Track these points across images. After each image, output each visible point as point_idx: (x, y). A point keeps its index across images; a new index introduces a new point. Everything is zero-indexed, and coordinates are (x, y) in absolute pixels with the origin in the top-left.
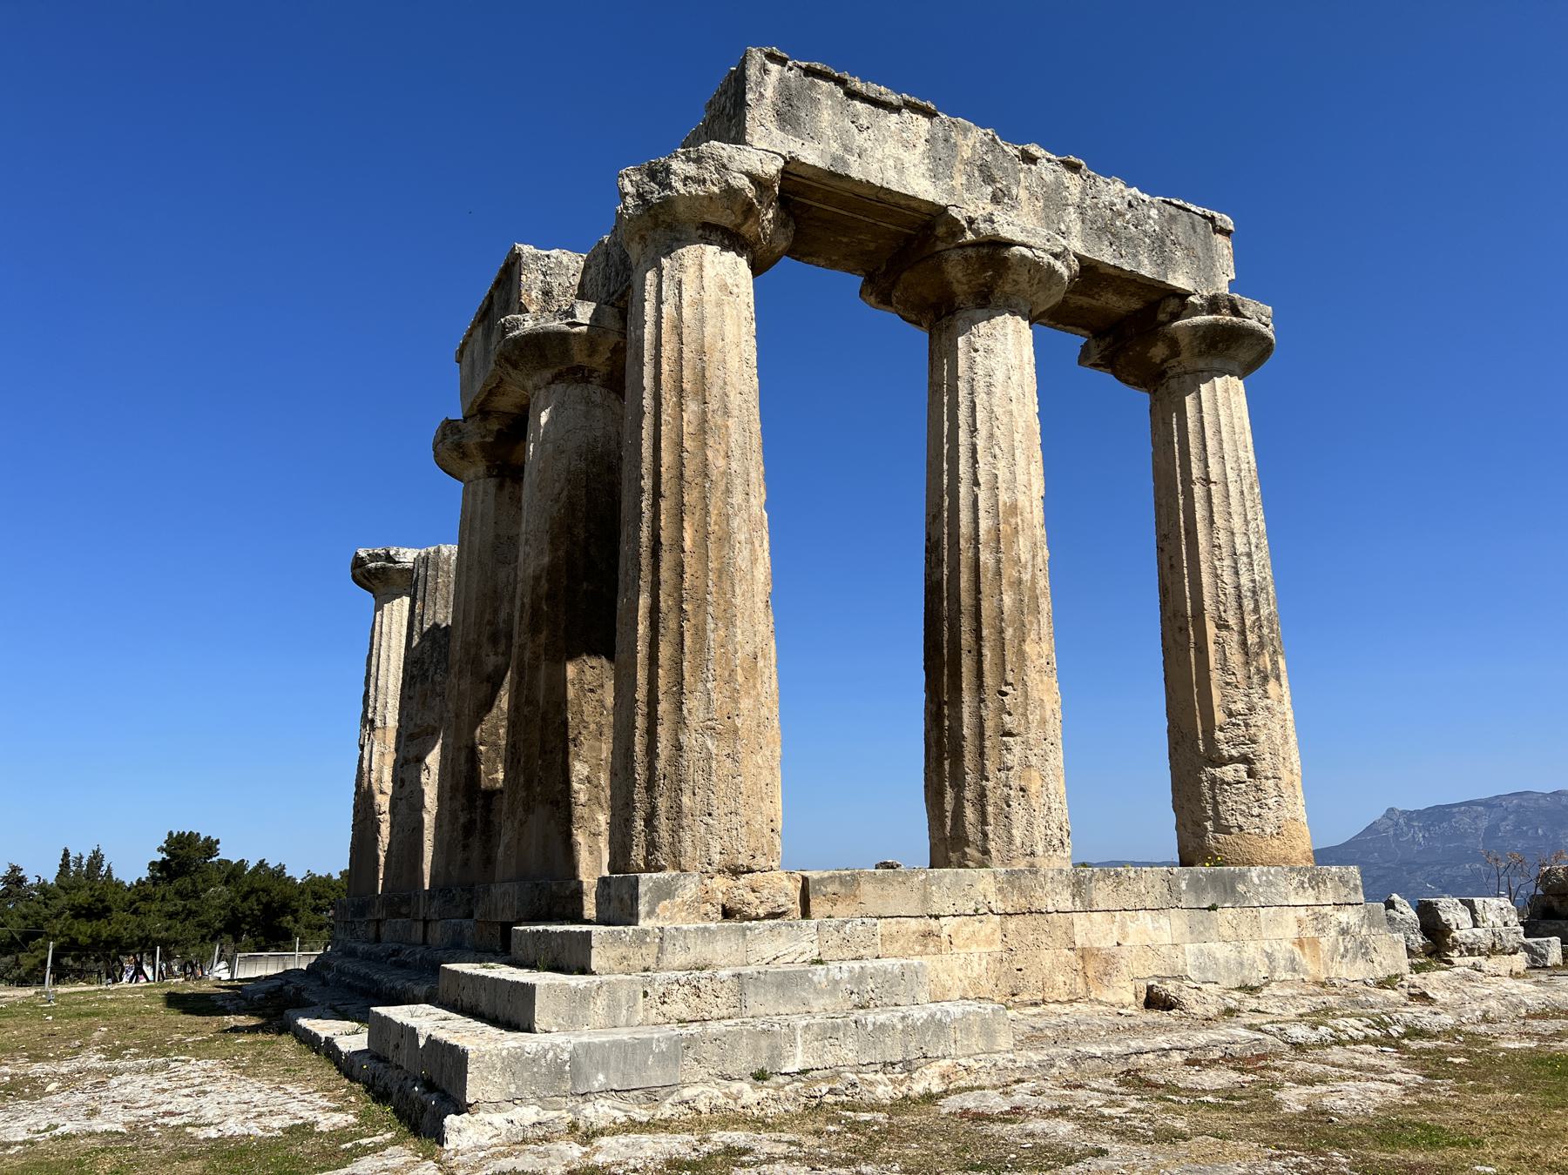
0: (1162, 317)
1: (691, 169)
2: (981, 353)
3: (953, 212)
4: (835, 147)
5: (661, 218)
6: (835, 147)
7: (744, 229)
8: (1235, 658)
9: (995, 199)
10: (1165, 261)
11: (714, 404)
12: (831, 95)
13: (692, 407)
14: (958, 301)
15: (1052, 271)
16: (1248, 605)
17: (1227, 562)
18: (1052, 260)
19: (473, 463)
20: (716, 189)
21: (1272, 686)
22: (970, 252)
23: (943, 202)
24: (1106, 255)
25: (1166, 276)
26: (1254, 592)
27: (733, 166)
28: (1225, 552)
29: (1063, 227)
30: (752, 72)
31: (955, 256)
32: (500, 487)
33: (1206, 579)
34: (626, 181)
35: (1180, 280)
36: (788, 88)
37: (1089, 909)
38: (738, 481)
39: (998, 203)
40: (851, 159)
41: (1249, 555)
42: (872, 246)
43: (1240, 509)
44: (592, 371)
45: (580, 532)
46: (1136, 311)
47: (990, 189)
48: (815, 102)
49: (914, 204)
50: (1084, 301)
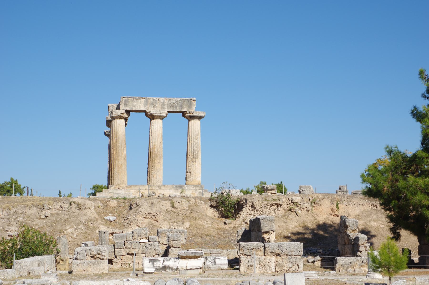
4: (131, 107)
8: (190, 160)
13: (115, 139)
16: (192, 153)
21: (194, 163)
35: (184, 110)
37: (160, 189)
48: (129, 102)
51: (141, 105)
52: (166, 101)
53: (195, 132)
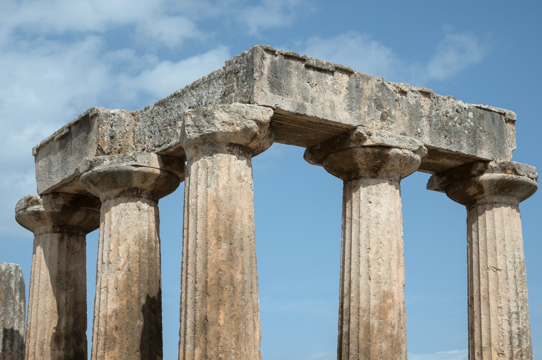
0: (474, 172)
1: (225, 117)
2: (373, 204)
3: (360, 130)
4: (299, 99)
5: (208, 140)
6: (299, 99)
7: (250, 145)
9: (383, 118)
10: (476, 144)
11: (236, 244)
12: (297, 68)
14: (361, 172)
15: (412, 159)
16: (516, 342)
17: (506, 317)
18: (412, 154)
19: (44, 224)
20: (238, 128)
22: (368, 150)
23: (355, 124)
24: (443, 144)
25: (476, 151)
26: (519, 335)
27: (249, 116)
28: (505, 311)
29: (419, 130)
30: (257, 60)
31: (360, 151)
32: (61, 239)
33: (493, 326)
34: (189, 118)
35: (484, 154)
36: (275, 67)
38: (247, 286)
39: (384, 120)
40: (307, 104)
41: (517, 313)
42: (314, 138)
43: (514, 286)
44: (142, 190)
45: (135, 289)
46: (460, 166)
47: (380, 113)
48: (289, 73)
49: (339, 125)
50: (431, 161)
51: (335, 98)
52: (426, 103)
53: (517, 253)
